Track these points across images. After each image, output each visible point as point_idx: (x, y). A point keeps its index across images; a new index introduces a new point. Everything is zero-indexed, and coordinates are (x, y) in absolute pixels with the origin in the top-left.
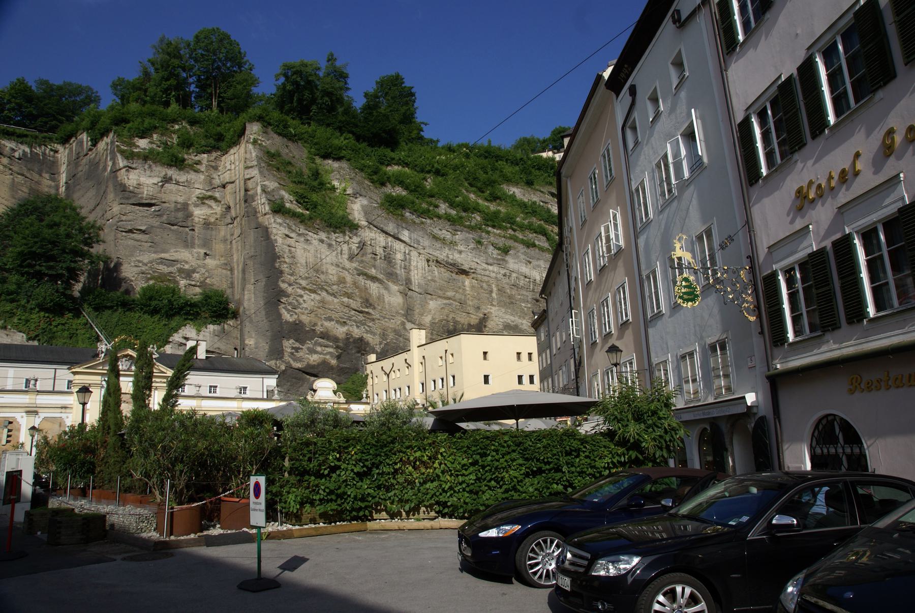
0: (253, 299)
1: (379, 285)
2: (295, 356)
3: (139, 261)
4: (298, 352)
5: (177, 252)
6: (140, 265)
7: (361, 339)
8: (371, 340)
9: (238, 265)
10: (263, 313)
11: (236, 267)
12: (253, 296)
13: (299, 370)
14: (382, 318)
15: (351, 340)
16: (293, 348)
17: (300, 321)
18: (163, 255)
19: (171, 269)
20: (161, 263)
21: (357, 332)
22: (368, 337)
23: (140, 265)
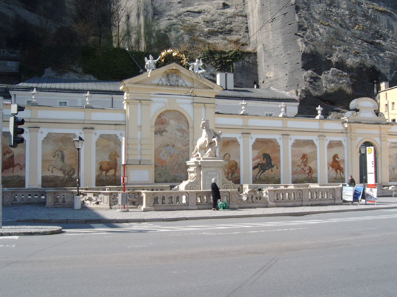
0: (271, 36)
1: (388, 17)
2: (314, 85)
3: (171, 15)
4: (316, 81)
5: (200, 4)
6: (172, 18)
7: (373, 68)
8: (383, 71)
9: (253, 11)
10: (282, 47)
11: (250, 13)
12: (271, 33)
13: (317, 97)
14: (392, 49)
15: (364, 70)
16: (311, 78)
17: (317, 53)
18: (189, 9)
19: (196, 20)
20: (188, 15)
21: (369, 62)
22: (380, 67)
23: (172, 18)
